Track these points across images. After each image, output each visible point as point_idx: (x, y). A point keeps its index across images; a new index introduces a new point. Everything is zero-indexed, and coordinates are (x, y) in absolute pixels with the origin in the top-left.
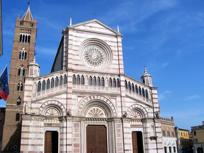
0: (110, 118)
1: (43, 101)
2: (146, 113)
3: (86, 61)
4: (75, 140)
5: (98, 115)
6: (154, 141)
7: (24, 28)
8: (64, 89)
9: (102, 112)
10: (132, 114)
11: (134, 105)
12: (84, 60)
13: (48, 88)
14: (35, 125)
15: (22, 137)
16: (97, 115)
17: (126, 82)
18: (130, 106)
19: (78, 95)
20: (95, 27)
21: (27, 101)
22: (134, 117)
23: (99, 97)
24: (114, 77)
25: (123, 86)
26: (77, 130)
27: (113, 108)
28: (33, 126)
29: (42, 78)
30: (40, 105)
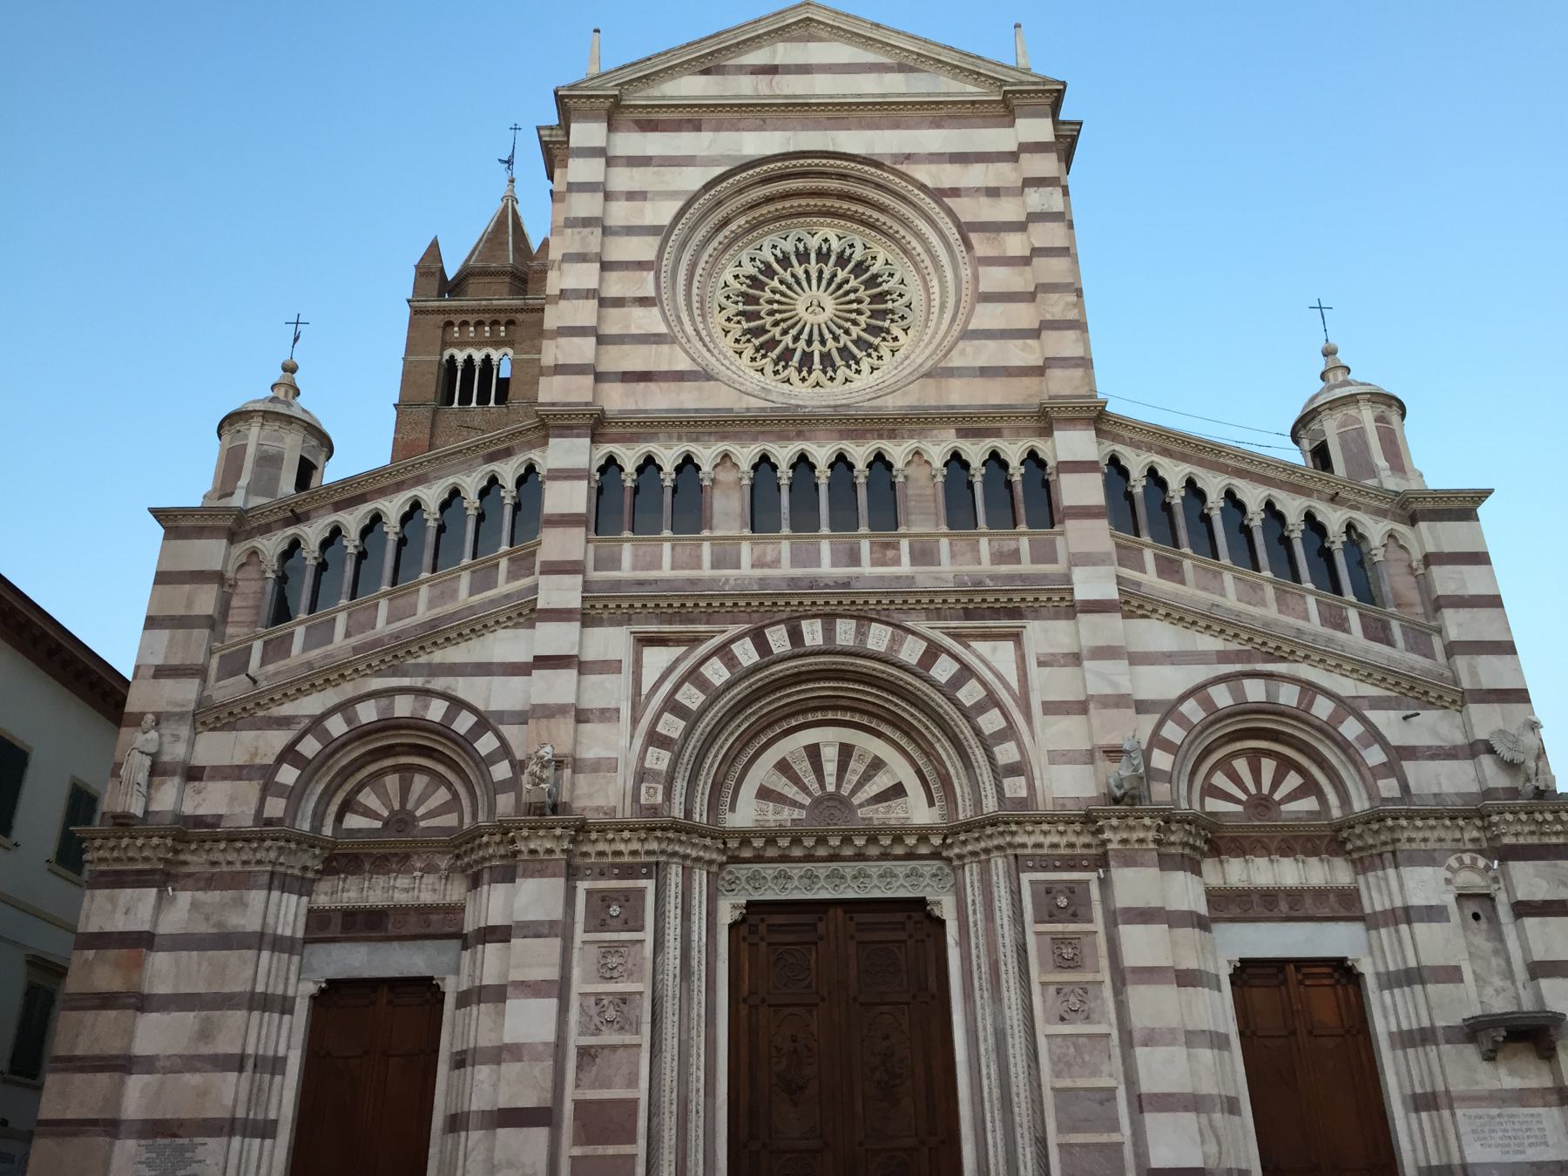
1: (312, 705)
3: (759, 363)
4: (594, 1057)
7: (466, 311)
9: (829, 744)
10: (1220, 780)
17: (1124, 473)
18: (1183, 698)
22: (1239, 808)
23: (845, 633)
24: (989, 443)
30: (278, 740)
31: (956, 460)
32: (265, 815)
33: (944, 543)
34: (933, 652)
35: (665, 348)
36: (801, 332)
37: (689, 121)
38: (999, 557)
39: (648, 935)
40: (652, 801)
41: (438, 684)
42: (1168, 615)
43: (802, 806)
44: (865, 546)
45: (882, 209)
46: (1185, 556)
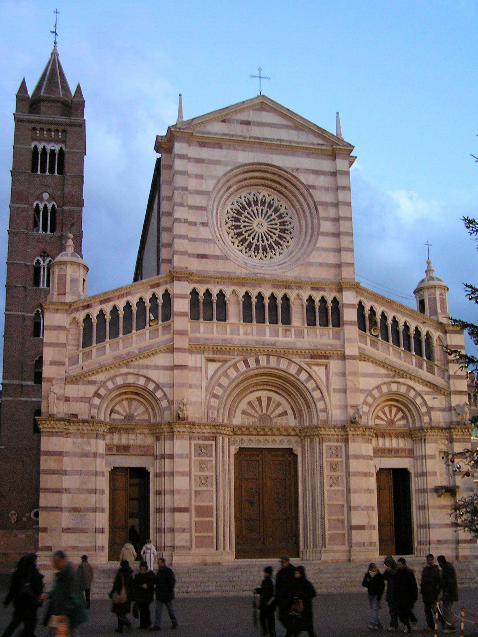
0: (308, 428)
1: (101, 377)
2: (424, 410)
3: (233, 240)
5: (272, 416)
6: (446, 501)
8: (162, 338)
10: (381, 414)
11: (385, 383)
12: (228, 239)
13: (114, 334)
14: (78, 450)
15: (42, 485)
16: (269, 416)
18: (373, 389)
19: (206, 355)
20: (260, 124)
21: (54, 378)
22: (384, 423)
25: (351, 323)
26: (204, 466)
27: (316, 394)
28: (74, 455)
29: (96, 304)
30: (91, 389)
31: (311, 300)
33: (306, 330)
34: (301, 369)
35: (212, 245)
36: (255, 236)
37: (218, 144)
39: (214, 459)
40: (213, 416)
42: (372, 361)
44: (280, 329)
45: (285, 187)
46: (379, 340)
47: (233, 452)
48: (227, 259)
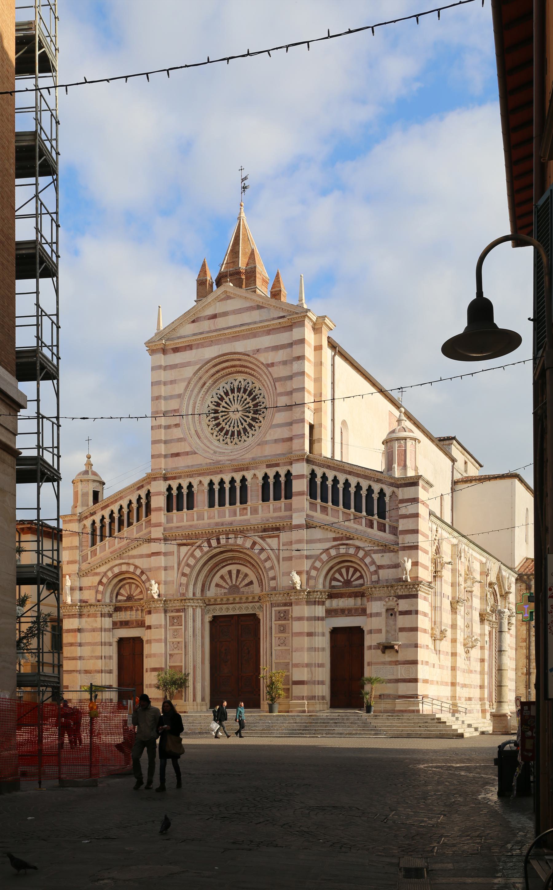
1: (103, 569)
10: (337, 576)
11: (332, 547)
12: (207, 431)
18: (321, 554)
22: (341, 584)
29: (99, 511)
30: (97, 579)
32: (98, 599)
33: (260, 507)
34: (254, 543)
35: (183, 443)
38: (275, 510)
39: (183, 627)
40: (183, 592)
41: (131, 561)
43: (226, 589)
45: (254, 370)
46: (329, 506)
47: (208, 618)
48: (195, 453)
